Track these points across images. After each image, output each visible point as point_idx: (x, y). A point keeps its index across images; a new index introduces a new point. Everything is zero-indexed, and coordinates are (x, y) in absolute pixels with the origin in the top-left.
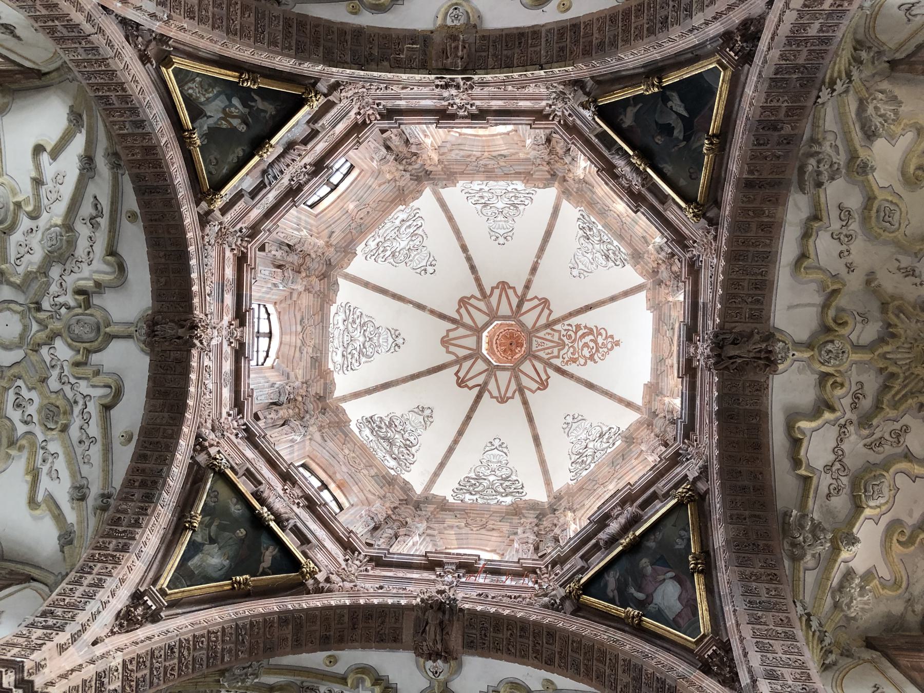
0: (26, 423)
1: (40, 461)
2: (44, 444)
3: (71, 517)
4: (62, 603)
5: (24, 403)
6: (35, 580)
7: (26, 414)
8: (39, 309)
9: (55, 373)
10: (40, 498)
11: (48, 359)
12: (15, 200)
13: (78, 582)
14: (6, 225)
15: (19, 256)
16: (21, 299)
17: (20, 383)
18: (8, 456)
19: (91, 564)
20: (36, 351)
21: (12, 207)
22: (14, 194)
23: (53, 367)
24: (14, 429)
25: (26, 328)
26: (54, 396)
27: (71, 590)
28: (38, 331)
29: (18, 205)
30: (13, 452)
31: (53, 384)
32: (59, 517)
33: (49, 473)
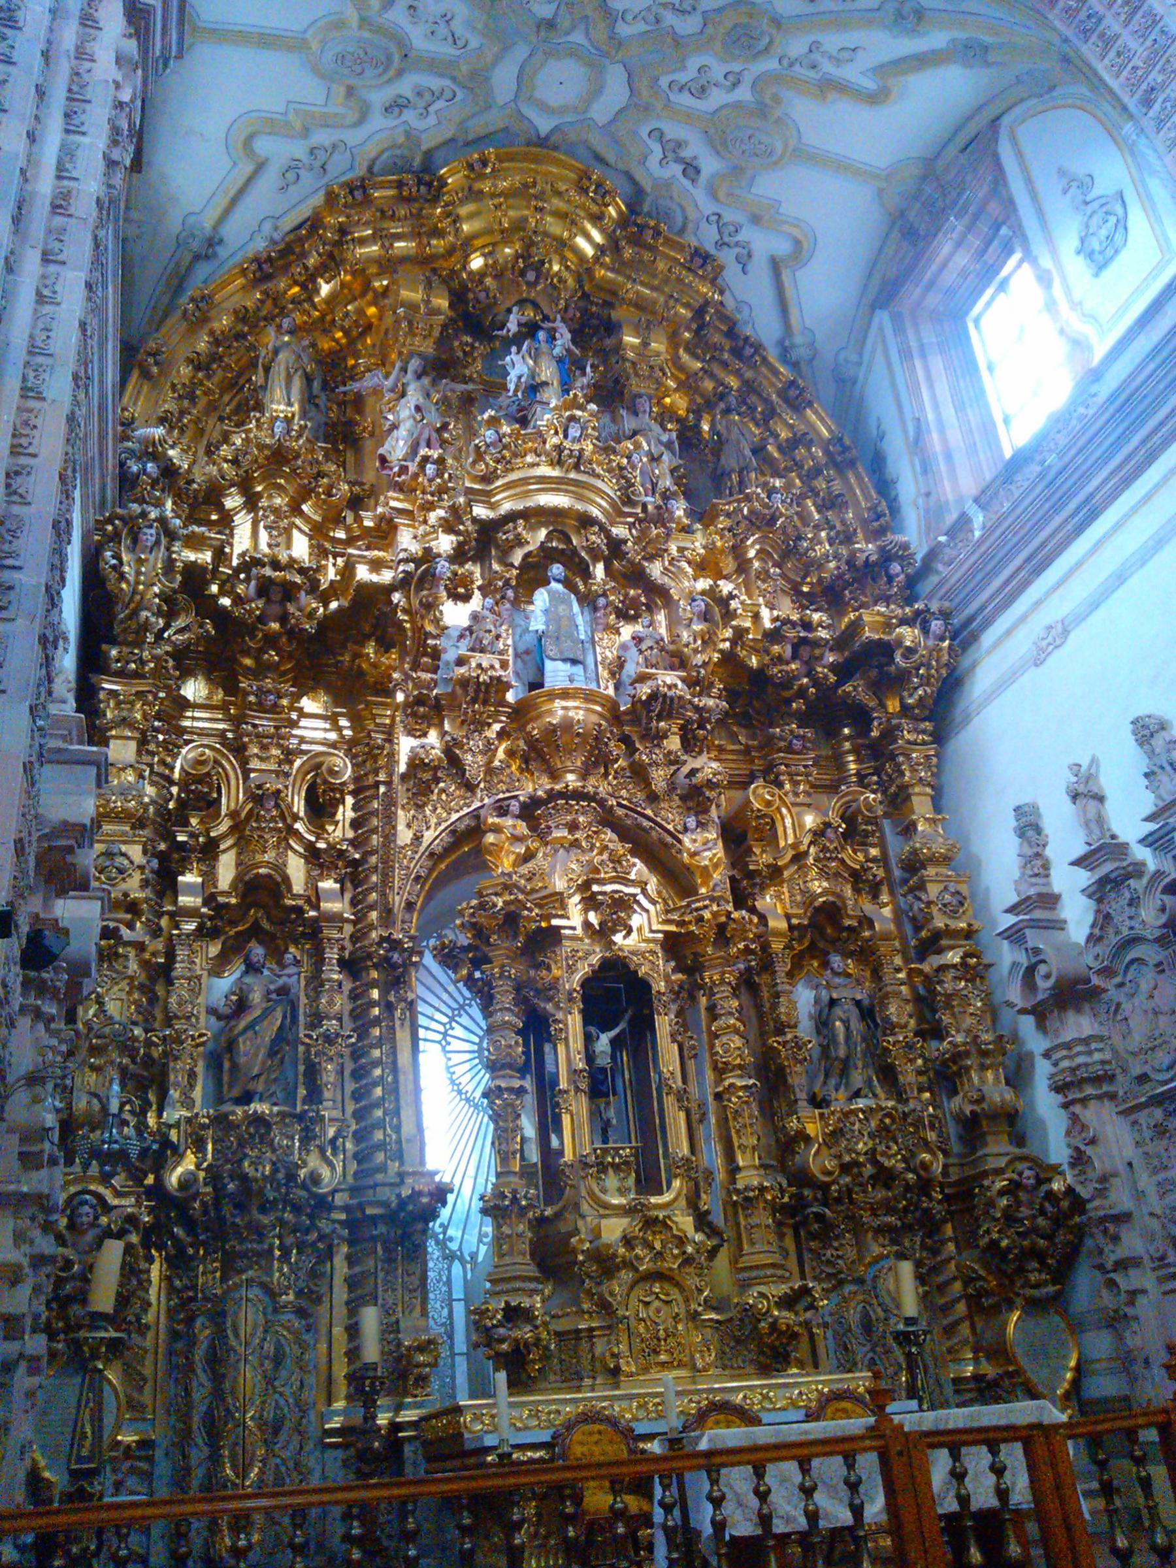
0: (735, 85)
1: (812, 74)
2: (785, 62)
3: (936, 39)
4: (1140, 73)
5: (703, 82)
6: (998, 118)
7: (721, 79)
8: (550, 24)
9: (670, 19)
10: (869, 84)
11: (642, 27)
12: (355, 25)
13: (1108, 42)
14: (393, 49)
15: (450, 39)
16: (521, 52)
17: (664, 82)
18: (778, 121)
19: (1083, 15)
20: (620, 44)
21: (366, 34)
22: (339, 24)
23: (657, 21)
24: (737, 105)
25: (574, 53)
26: (710, 30)
27: (1119, 54)
28: (587, 34)
29: (364, 22)
30: (777, 113)
31: (688, 26)
32: (922, 61)
33: (838, 62)
